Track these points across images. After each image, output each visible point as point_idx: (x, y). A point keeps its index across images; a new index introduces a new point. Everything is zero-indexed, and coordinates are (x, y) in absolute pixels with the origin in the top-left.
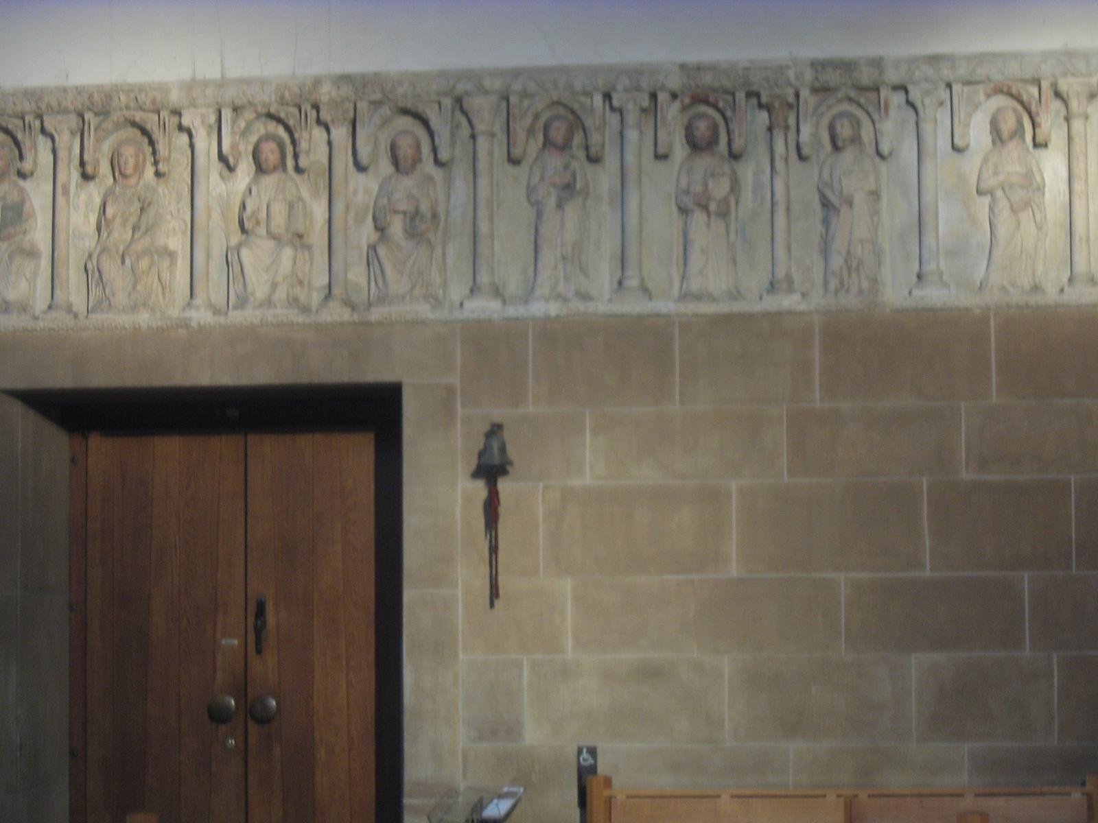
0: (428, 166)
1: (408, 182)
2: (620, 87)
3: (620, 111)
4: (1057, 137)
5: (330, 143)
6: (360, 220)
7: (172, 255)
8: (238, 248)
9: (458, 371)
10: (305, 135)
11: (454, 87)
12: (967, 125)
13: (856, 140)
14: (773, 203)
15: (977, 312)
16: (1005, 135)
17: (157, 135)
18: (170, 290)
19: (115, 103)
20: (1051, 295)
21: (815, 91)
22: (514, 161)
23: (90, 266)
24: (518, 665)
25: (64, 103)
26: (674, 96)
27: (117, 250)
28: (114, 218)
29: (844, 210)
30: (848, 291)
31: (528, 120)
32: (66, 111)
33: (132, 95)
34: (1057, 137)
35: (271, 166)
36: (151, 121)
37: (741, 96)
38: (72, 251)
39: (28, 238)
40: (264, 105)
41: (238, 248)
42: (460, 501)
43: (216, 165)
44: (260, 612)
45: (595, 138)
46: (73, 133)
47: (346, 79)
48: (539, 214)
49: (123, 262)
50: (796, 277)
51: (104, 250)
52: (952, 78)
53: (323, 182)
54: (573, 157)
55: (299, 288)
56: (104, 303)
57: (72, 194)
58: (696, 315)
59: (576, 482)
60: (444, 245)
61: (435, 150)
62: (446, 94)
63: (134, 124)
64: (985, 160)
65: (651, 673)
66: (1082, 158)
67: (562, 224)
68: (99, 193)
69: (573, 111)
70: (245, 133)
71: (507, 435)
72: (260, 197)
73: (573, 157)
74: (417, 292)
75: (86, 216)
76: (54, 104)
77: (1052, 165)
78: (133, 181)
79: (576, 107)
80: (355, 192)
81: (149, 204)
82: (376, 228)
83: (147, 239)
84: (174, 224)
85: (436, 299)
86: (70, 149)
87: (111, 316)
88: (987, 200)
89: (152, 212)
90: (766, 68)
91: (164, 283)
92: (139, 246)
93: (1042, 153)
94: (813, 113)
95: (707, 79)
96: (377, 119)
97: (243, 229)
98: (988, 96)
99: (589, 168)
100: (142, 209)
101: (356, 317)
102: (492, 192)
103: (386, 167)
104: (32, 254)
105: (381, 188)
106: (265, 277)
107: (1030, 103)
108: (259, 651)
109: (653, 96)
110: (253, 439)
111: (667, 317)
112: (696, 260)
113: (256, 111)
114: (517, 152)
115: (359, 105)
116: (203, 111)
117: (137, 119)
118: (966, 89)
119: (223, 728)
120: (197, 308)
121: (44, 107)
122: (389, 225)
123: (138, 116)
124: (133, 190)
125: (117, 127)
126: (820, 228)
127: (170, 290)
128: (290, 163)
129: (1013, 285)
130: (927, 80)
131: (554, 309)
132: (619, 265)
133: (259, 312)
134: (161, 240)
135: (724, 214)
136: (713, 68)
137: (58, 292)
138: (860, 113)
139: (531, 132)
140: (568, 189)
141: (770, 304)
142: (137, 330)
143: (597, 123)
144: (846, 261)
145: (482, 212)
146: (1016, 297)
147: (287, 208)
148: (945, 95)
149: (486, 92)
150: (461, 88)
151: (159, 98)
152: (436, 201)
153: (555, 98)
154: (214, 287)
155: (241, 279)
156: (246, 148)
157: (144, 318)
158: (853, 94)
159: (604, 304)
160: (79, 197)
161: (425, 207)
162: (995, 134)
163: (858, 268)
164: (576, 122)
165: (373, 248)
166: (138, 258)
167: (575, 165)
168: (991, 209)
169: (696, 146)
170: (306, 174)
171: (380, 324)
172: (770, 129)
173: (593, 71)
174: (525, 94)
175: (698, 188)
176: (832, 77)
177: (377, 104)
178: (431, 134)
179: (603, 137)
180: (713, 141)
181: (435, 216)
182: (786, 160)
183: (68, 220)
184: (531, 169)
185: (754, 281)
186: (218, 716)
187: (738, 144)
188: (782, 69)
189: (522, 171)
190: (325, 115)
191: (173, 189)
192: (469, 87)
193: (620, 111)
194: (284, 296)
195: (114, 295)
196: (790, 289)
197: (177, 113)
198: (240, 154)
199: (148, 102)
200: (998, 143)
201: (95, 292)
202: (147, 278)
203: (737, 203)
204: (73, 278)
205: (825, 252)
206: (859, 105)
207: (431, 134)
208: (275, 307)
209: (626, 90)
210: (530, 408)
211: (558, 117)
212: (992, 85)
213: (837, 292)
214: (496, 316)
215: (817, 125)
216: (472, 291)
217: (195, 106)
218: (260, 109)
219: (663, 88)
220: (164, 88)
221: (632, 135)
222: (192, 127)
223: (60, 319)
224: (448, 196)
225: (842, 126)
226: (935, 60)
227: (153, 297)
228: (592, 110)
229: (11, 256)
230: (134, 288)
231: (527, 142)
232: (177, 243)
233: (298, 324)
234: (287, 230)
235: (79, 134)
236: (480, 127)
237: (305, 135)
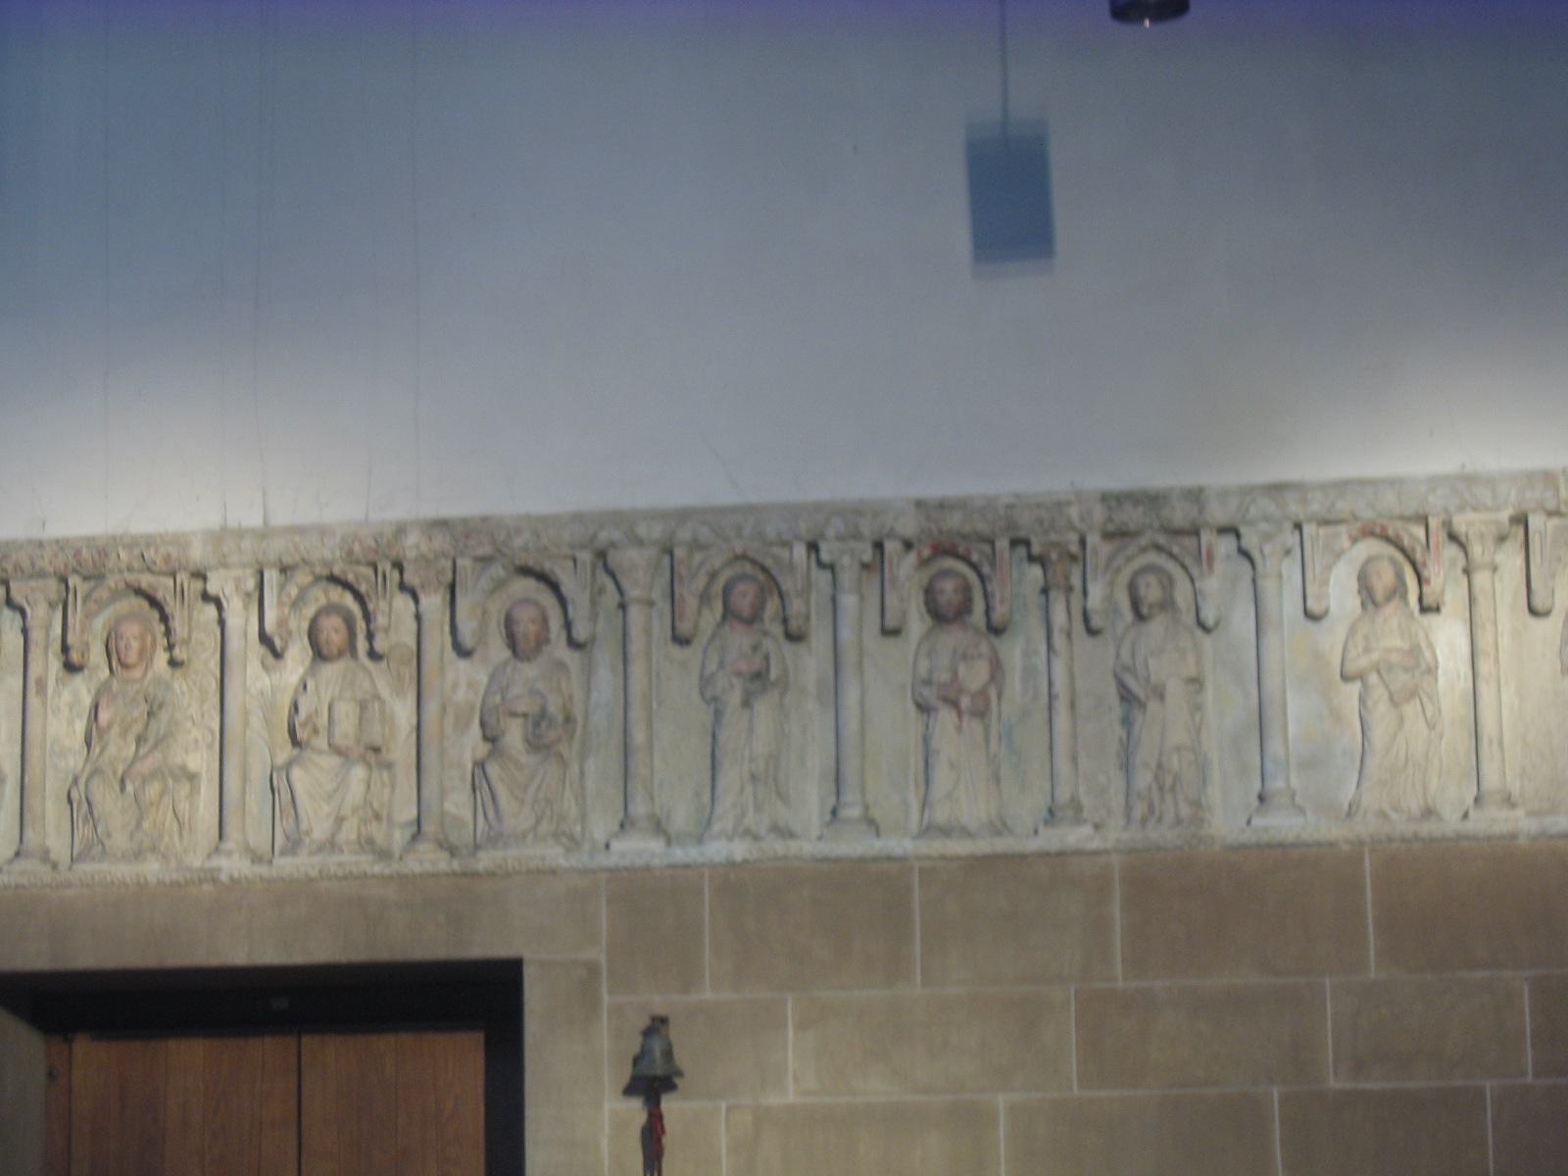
0: (559, 649)
1: (529, 671)
2: (831, 533)
3: (831, 567)
4: (1453, 597)
5: (418, 617)
6: (462, 725)
7: (193, 777)
8: (288, 766)
9: (604, 942)
10: (383, 605)
11: (594, 537)
12: (1325, 582)
13: (1167, 604)
14: (1051, 697)
15: (1346, 848)
16: (1379, 596)
17: (172, 606)
18: (190, 829)
19: (111, 563)
20: (1450, 822)
21: (1108, 536)
22: (681, 640)
23: (75, 795)
25: (39, 563)
26: (908, 545)
27: (115, 773)
28: (110, 726)
29: (1153, 706)
30: (1160, 820)
31: (701, 582)
33: (136, 552)
34: (1453, 597)
35: (335, 652)
36: (163, 588)
37: (1003, 544)
38: (50, 773)
40: (325, 563)
41: (288, 766)
42: (607, 1130)
43: (257, 650)
45: (796, 606)
46: (52, 605)
47: (443, 524)
48: (718, 715)
49: (123, 788)
50: (1086, 801)
51: (96, 772)
52: (1302, 516)
53: (409, 672)
54: (765, 633)
55: (374, 824)
56: (94, 848)
57: (50, 692)
58: (943, 857)
59: (772, 1100)
60: (583, 758)
61: (568, 625)
62: (583, 547)
63: (139, 592)
64: (1352, 631)
66: (1489, 627)
67: (751, 730)
68: (89, 691)
69: (764, 569)
70: (297, 604)
71: (674, 1033)
72: (319, 697)
73: (765, 633)
74: (544, 828)
75: (71, 723)
76: (26, 564)
77: (1447, 637)
78: (137, 673)
79: (769, 562)
80: (455, 686)
81: (161, 706)
82: (486, 738)
83: (158, 755)
84: (196, 733)
85: (571, 838)
86: (48, 628)
87: (104, 866)
88: (1355, 688)
89: (164, 716)
90: (1038, 506)
91: (181, 820)
92: (144, 766)
93: (1431, 619)
94: (1108, 566)
95: (954, 521)
96: (485, 583)
97: (295, 741)
98: (1354, 540)
99: (788, 648)
100: (150, 714)
101: (456, 865)
102: (650, 689)
103: (498, 651)
105: (492, 678)
106: (326, 809)
107: (1414, 550)
109: (879, 546)
110: (309, 1041)
111: (903, 859)
112: (942, 777)
113: (313, 573)
114: (685, 627)
115: (459, 562)
116: (237, 572)
117: (144, 585)
118: (1322, 531)
120: (229, 854)
122: (503, 733)
123: (145, 580)
124: (136, 687)
125: (115, 596)
126: (1119, 731)
127: (190, 829)
128: (362, 645)
129: (1395, 809)
130: (1267, 519)
131: (740, 850)
132: (833, 788)
133: (317, 859)
134: (177, 757)
135: (981, 713)
136: (962, 505)
137: (29, 833)
138: (1171, 566)
139: (704, 598)
140: (759, 677)
141: (1051, 839)
142: (142, 886)
143: (799, 586)
144: (1156, 778)
145: (637, 713)
146: (1400, 826)
147: (358, 710)
148: (1292, 539)
149: (640, 543)
150: (604, 536)
151: (174, 552)
152: (571, 698)
153: (739, 551)
154: (254, 824)
155: (292, 811)
156: (300, 624)
157: (152, 869)
158: (1162, 540)
159: (811, 843)
160: (60, 696)
161: (554, 707)
162: (1364, 593)
163: (1173, 788)
164: (769, 583)
165: (480, 765)
166: (144, 782)
167: (768, 644)
168: (1362, 700)
169: (940, 616)
170: (385, 662)
171: (491, 874)
172: (1045, 591)
173: (792, 511)
174: (696, 545)
175: (944, 676)
176: (1132, 516)
177: (485, 561)
178: (563, 602)
179: (807, 603)
180: (964, 609)
181: (569, 719)
182: (1069, 635)
183: (44, 727)
184: (705, 651)
185: (1027, 807)
187: (999, 612)
188: (1060, 505)
189: (692, 654)
190: (411, 578)
191: (194, 683)
192: (616, 535)
193: (831, 567)
194: (353, 836)
195: (109, 835)
196: (1078, 820)
197: (200, 575)
198: (290, 633)
199: (159, 560)
200: (1370, 606)
201: (83, 831)
202: (157, 811)
203: (999, 696)
204: (51, 812)
205: (1127, 767)
206: (1171, 555)
207: (563, 602)
208: (341, 851)
209: (840, 538)
211: (743, 577)
212: (1359, 525)
213: (1144, 821)
214: (656, 862)
215: (1112, 584)
216: (622, 826)
217: (224, 565)
218: (318, 570)
219: (892, 535)
220: (180, 540)
221: (848, 601)
222: (222, 596)
224: (588, 691)
225: (1148, 585)
226: (1276, 489)
227: (166, 839)
228: (791, 567)
230: (138, 825)
231: (699, 613)
232: (200, 760)
233: (374, 876)
234: (358, 741)
235: (61, 607)
236: (633, 592)
237: (383, 605)
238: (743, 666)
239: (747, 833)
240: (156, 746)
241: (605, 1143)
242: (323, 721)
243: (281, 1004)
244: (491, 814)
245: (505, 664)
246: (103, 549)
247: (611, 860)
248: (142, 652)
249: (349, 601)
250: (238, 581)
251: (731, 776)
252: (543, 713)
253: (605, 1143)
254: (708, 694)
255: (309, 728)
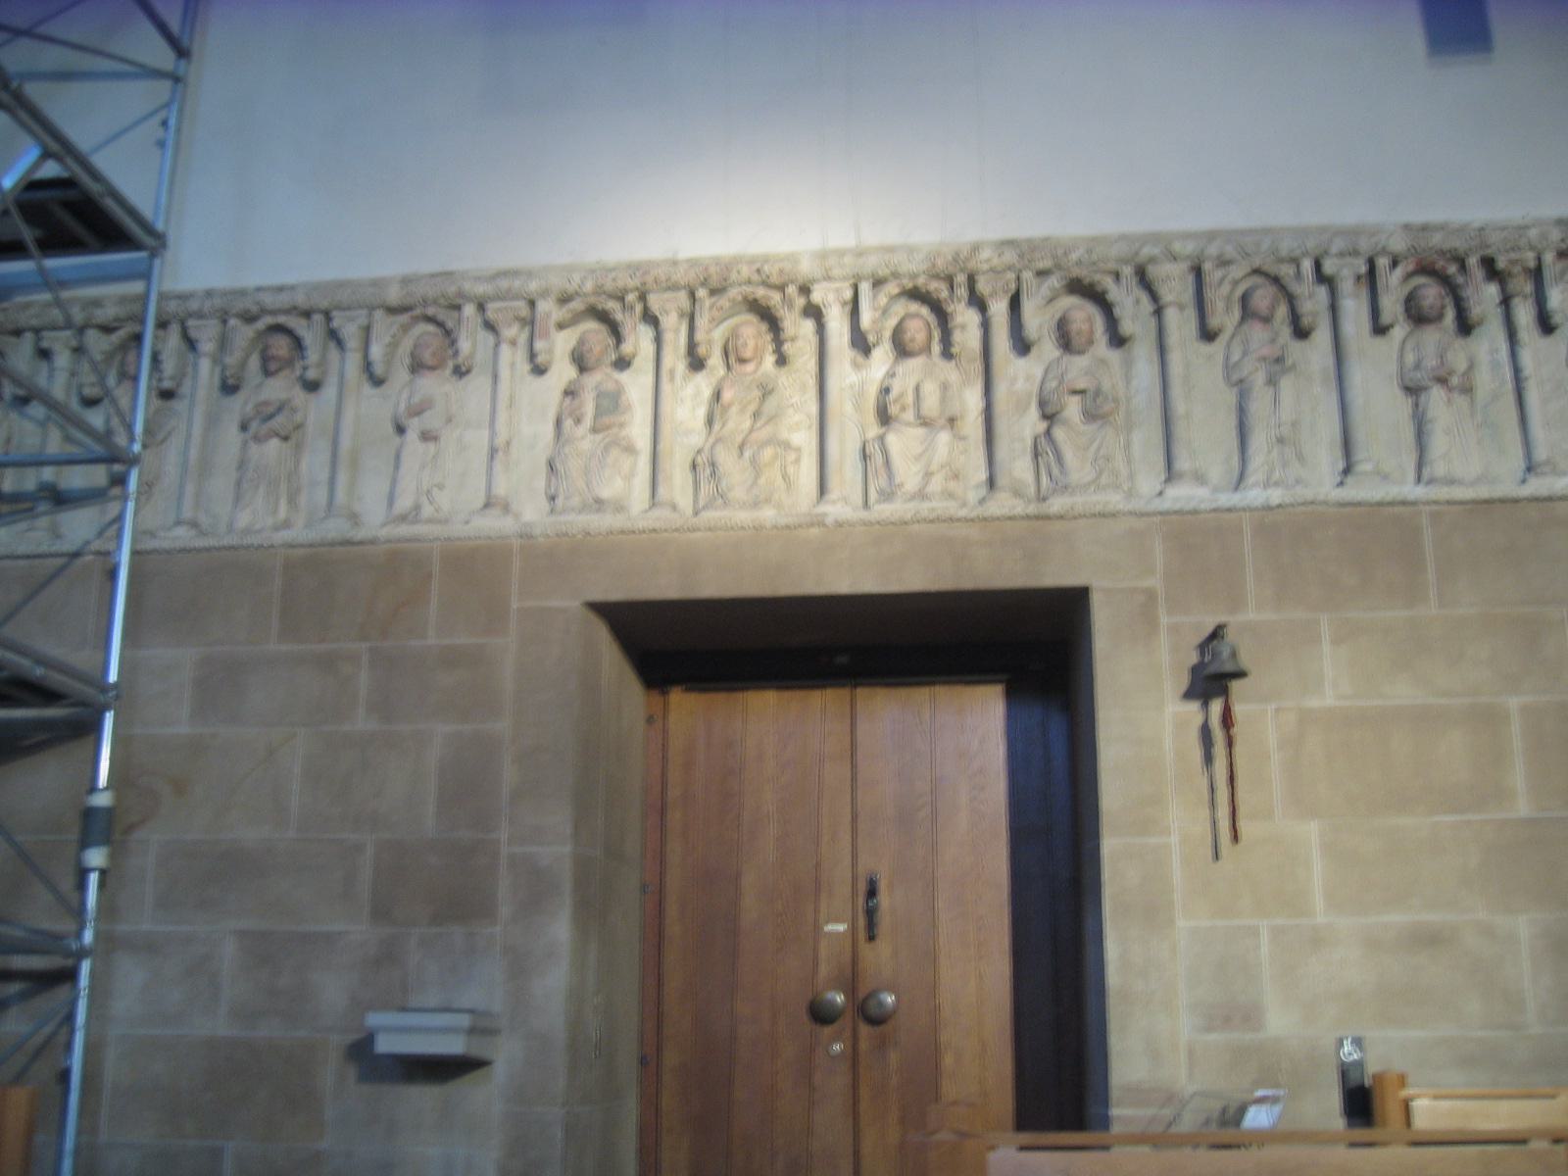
2: (1334, 249)
6: (1021, 408)
7: (798, 450)
19: (734, 276)
22: (1208, 335)
23: (699, 460)
24: (1254, 932)
25: (674, 278)
26: (1395, 263)
31: (1226, 289)
32: (674, 287)
33: (755, 267)
39: (624, 433)
40: (914, 276)
44: (872, 892)
46: (682, 315)
56: (721, 497)
58: (1449, 502)
59: (1313, 703)
62: (1126, 262)
65: (1429, 939)
67: (1276, 401)
69: (1276, 280)
70: (885, 311)
74: (1104, 480)
76: (663, 278)
78: (750, 367)
84: (797, 418)
90: (1503, 229)
92: (763, 434)
95: (1436, 240)
99: (1296, 348)
104: (630, 449)
108: (871, 938)
110: (862, 693)
111: (1414, 503)
112: (1438, 443)
116: (837, 285)
119: (827, 1030)
120: (834, 502)
121: (649, 279)
122: (1062, 409)
123: (760, 292)
124: (751, 378)
128: (936, 348)
131: (1276, 496)
133: (912, 505)
134: (784, 435)
136: (1442, 227)
137: (662, 491)
141: (1537, 486)
142: (758, 528)
149: (1175, 258)
150: (1147, 251)
151: (787, 266)
157: (768, 515)
161: (1106, 386)
172: (1506, 301)
173: (1303, 232)
174: (1223, 262)
177: (1042, 274)
181: (1116, 400)
184: (1228, 346)
186: (821, 1015)
189: (1217, 348)
190: (983, 286)
192: (1156, 251)
197: (805, 290)
209: (1341, 254)
210: (1251, 615)
217: (828, 278)
219: (1384, 251)
220: (793, 258)
223: (660, 517)
229: (606, 449)
230: (755, 483)
232: (804, 438)
233: (959, 520)
236: (1167, 295)
238: (1265, 351)
239: (1276, 484)
240: (767, 423)
241: (1168, 743)
242: (910, 399)
243: (842, 660)
244: (1056, 471)
245: (1058, 360)
246: (728, 265)
247: (1166, 504)
248: (756, 348)
249: (925, 311)
250: (837, 290)
251: (1259, 440)
252: (1098, 393)
253: (1168, 743)
254: (1235, 377)
255: (898, 407)
